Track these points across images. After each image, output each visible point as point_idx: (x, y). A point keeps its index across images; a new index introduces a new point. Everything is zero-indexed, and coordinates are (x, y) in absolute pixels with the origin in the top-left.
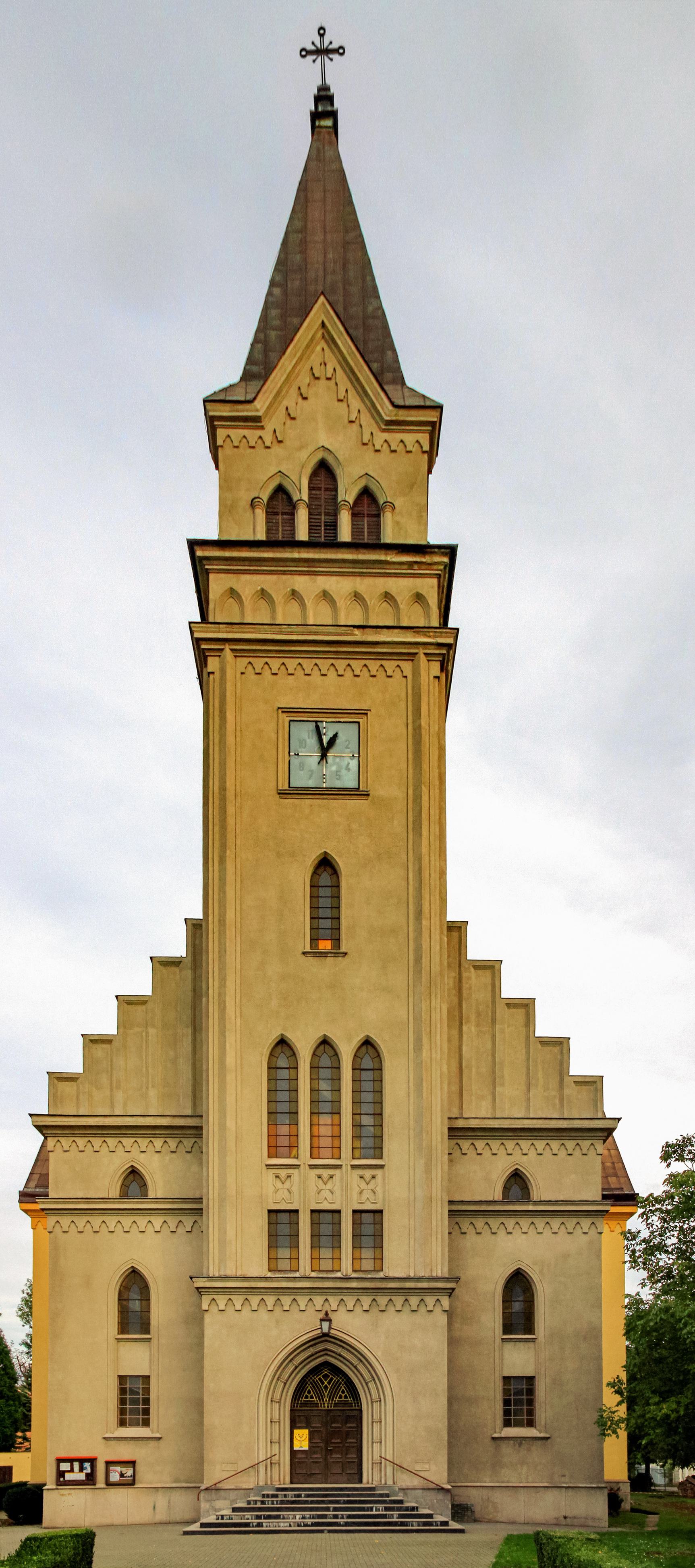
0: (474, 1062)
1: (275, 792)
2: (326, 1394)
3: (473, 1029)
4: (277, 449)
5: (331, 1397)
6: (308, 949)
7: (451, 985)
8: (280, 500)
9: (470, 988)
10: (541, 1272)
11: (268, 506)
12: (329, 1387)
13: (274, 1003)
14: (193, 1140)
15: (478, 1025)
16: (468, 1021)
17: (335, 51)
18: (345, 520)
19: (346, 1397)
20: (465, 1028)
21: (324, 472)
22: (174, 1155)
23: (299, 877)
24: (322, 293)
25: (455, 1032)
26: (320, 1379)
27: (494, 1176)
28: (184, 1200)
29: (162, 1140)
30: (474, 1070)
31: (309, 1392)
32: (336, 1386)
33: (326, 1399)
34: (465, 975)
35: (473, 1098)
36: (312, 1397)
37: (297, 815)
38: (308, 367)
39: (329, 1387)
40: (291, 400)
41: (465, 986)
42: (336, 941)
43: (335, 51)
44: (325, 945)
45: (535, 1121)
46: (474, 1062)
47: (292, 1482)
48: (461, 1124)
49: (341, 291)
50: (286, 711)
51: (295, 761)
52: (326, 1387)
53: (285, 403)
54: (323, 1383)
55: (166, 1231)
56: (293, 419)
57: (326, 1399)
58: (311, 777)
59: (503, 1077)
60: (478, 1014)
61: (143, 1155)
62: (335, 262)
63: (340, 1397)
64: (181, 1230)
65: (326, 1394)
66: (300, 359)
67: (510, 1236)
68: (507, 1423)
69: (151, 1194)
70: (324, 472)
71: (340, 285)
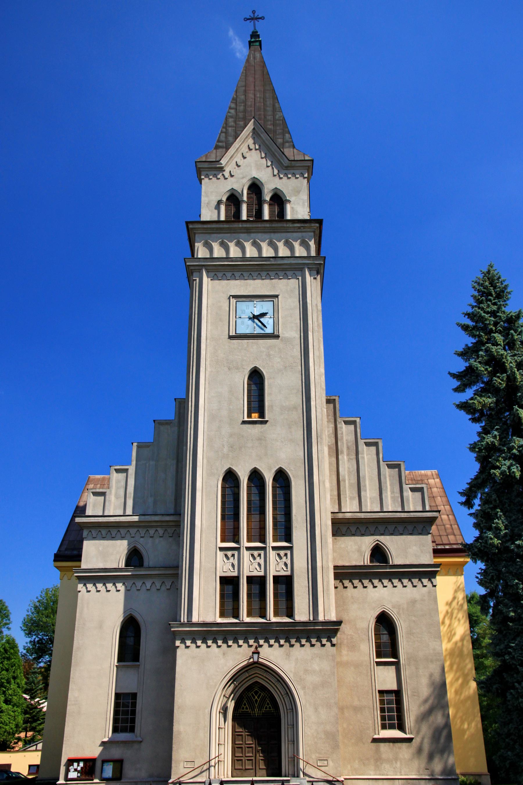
0: (347, 477)
1: (227, 337)
2: (256, 705)
3: (345, 457)
4: (230, 179)
5: (260, 707)
6: (246, 419)
7: (331, 431)
8: (233, 199)
9: (342, 434)
10: (398, 613)
11: (226, 203)
12: (259, 700)
13: (225, 450)
14: (174, 529)
15: (348, 455)
16: (342, 452)
17: (260, 18)
18: (266, 209)
19: (270, 708)
20: (340, 457)
21: (255, 187)
22: (161, 539)
23: (241, 380)
24: (254, 118)
25: (334, 459)
26: (252, 694)
27: (364, 548)
28: (166, 568)
29: (155, 529)
30: (347, 482)
31: (245, 705)
32: (263, 700)
33: (256, 710)
34: (338, 426)
35: (348, 499)
36: (247, 708)
37: (240, 347)
38: (246, 145)
39: (259, 700)
40: (238, 158)
41: (339, 432)
42: (262, 414)
43: (260, 18)
44: (255, 417)
45: (387, 514)
46: (347, 477)
47: (232, 776)
48: (340, 516)
49: (262, 110)
50: (234, 297)
51: (239, 321)
52: (256, 701)
53: (236, 160)
54: (254, 697)
55: (154, 589)
56: (240, 166)
57: (256, 710)
58: (248, 328)
59: (365, 486)
60: (348, 448)
61: (142, 539)
62: (260, 98)
63: (266, 708)
64: (163, 588)
65: (256, 705)
66: (243, 142)
67: (376, 589)
68: (384, 727)
69: (146, 564)
70: (255, 187)
71: (262, 107)
